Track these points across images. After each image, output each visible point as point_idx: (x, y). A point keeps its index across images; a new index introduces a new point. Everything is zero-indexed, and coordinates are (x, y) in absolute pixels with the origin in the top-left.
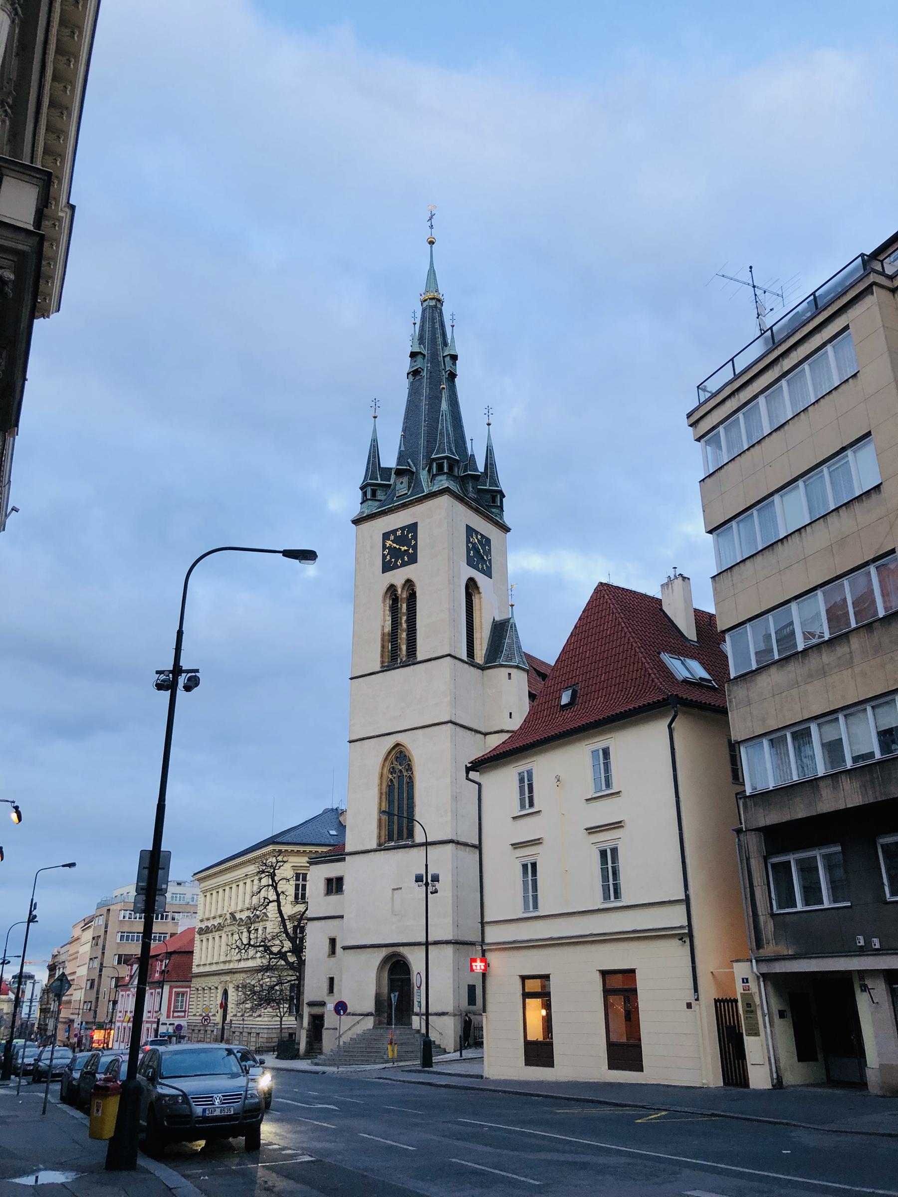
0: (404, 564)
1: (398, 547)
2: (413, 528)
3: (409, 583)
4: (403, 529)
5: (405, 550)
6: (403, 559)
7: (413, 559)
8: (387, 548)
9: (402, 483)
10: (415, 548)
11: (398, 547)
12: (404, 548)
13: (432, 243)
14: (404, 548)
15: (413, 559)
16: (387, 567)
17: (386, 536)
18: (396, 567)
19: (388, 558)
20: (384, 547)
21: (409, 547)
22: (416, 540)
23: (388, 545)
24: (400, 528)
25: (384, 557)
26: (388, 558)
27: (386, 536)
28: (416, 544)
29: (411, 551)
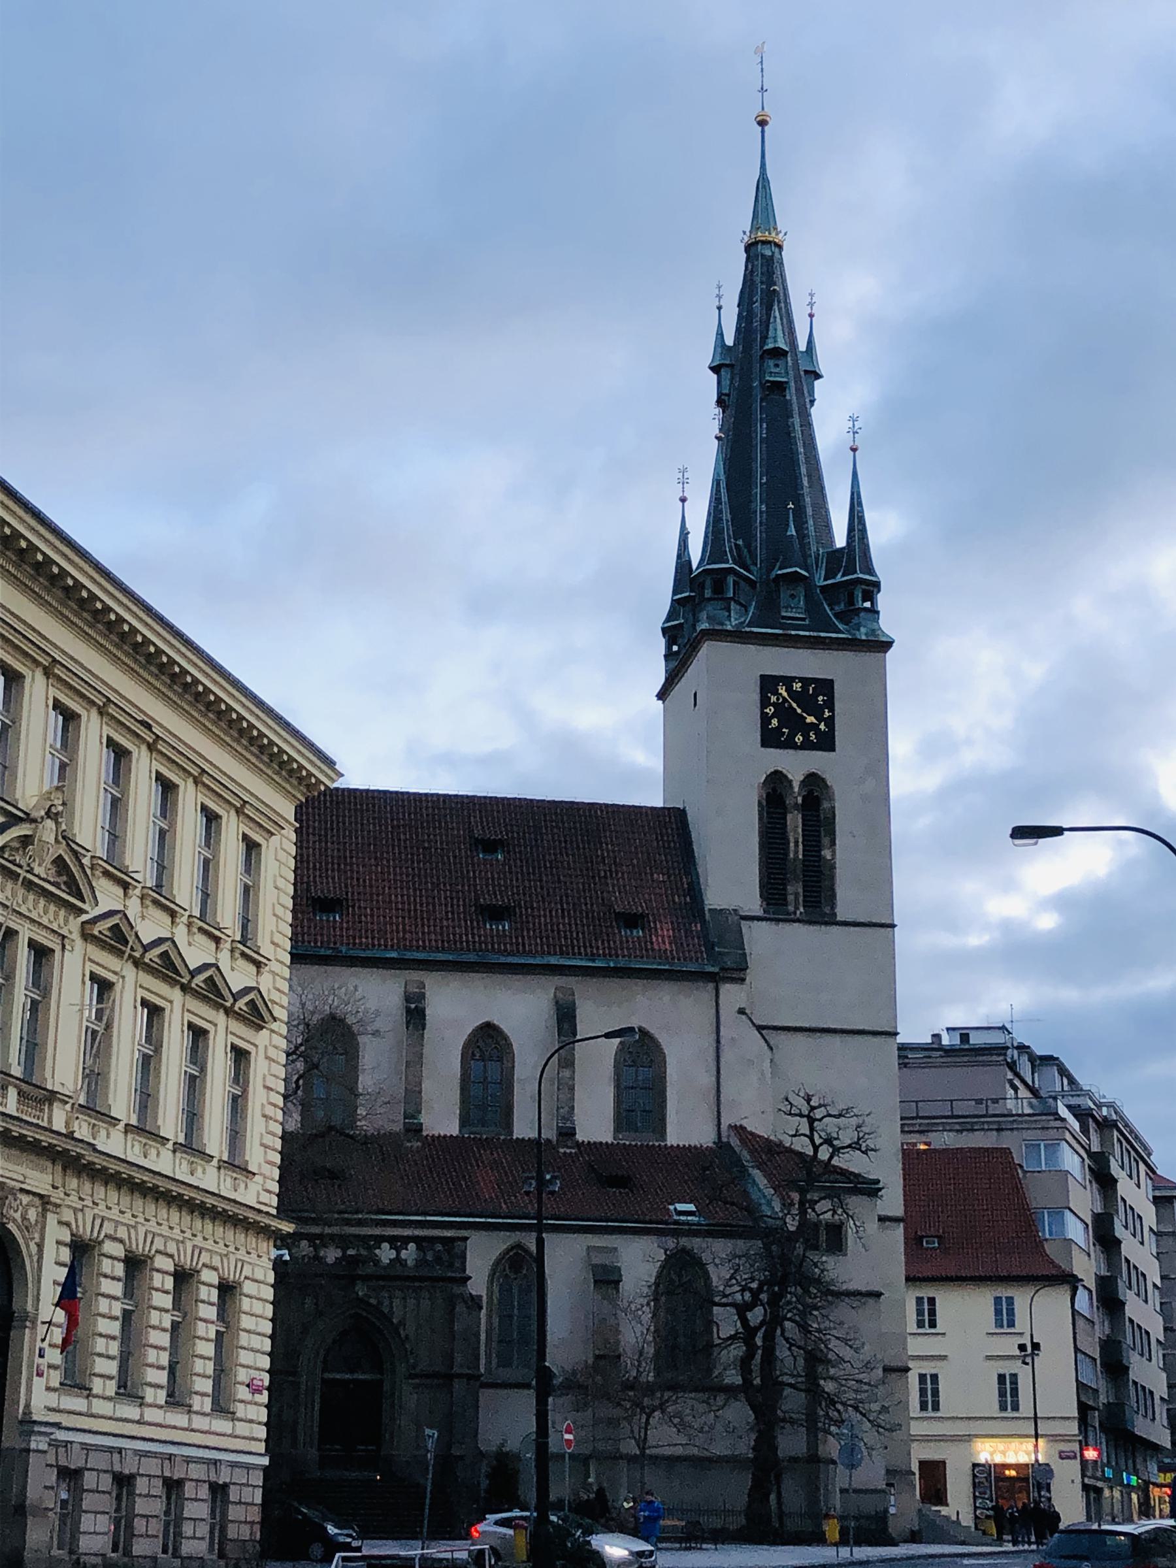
0: (807, 746)
1: (799, 711)
2: (826, 686)
3: (814, 782)
4: (806, 681)
5: (812, 723)
6: (806, 736)
7: (827, 743)
8: (774, 705)
9: (793, 596)
10: (830, 722)
11: (799, 711)
12: (810, 719)
13: (762, 123)
14: (810, 719)
15: (827, 743)
16: (770, 739)
17: (768, 683)
18: (790, 745)
19: (775, 722)
20: (765, 703)
21: (820, 718)
22: (832, 710)
23: (773, 699)
24: (801, 680)
25: (765, 719)
26: (775, 722)
27: (768, 683)
28: (832, 718)
29: (822, 727)
